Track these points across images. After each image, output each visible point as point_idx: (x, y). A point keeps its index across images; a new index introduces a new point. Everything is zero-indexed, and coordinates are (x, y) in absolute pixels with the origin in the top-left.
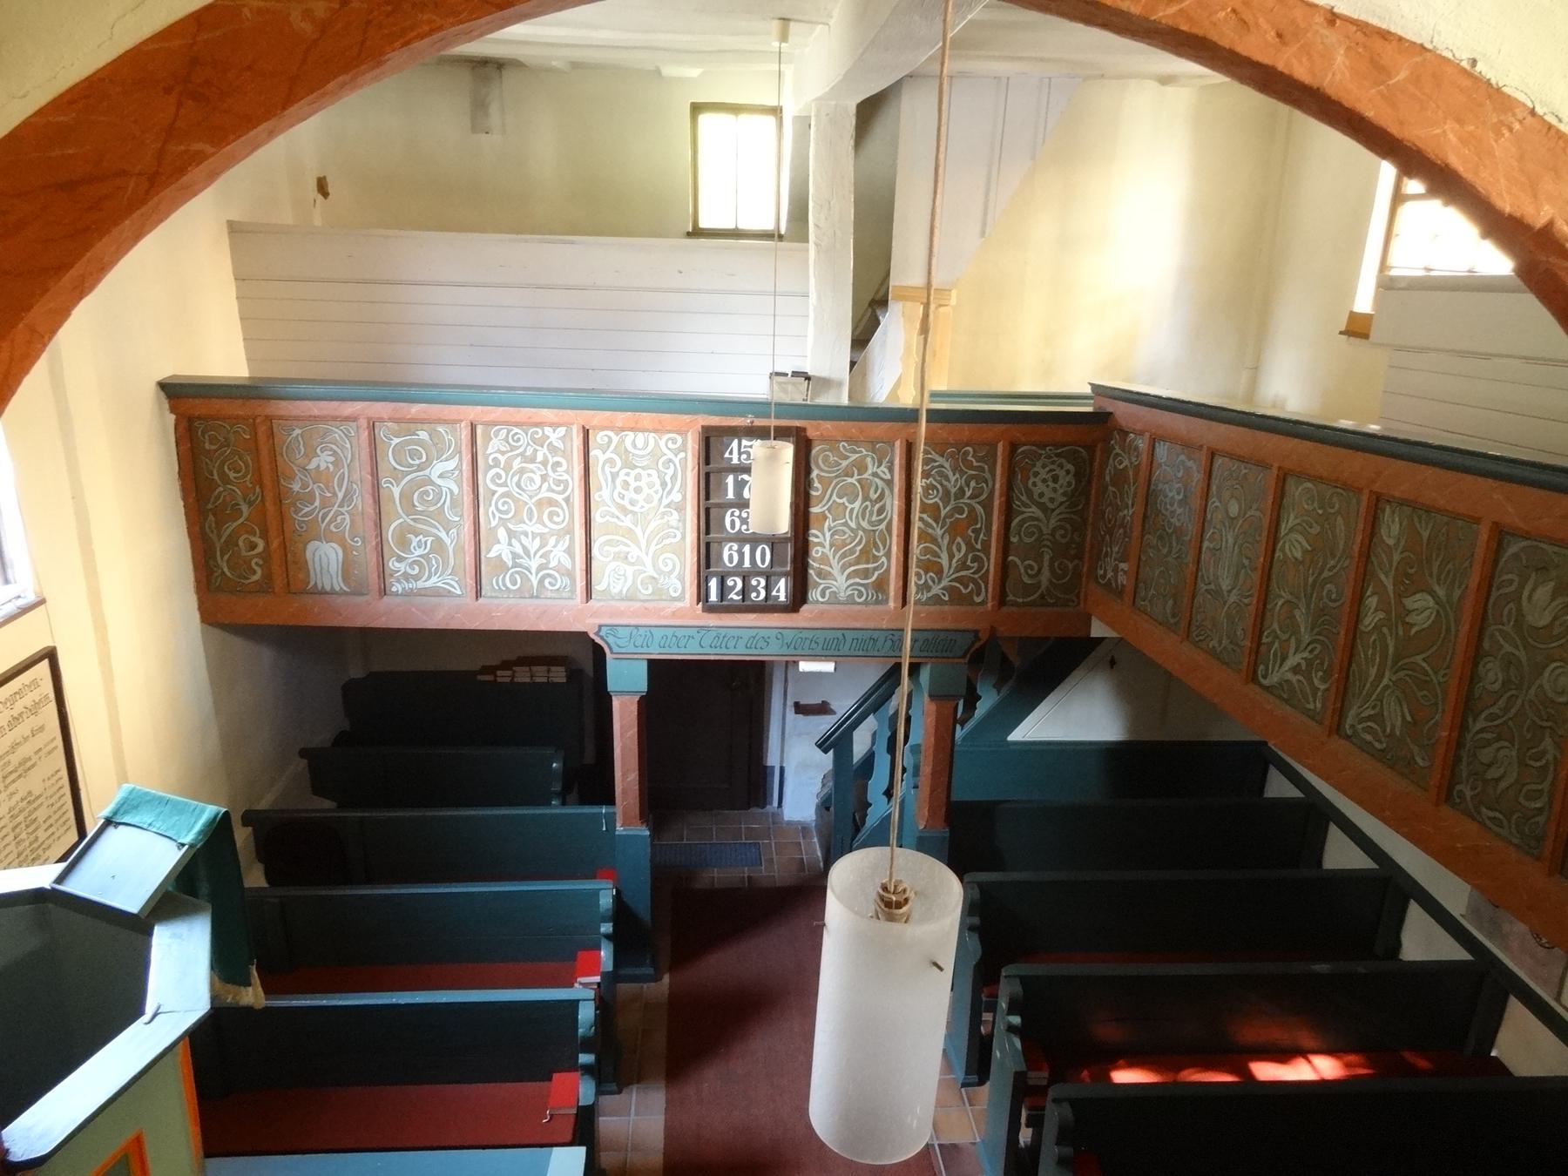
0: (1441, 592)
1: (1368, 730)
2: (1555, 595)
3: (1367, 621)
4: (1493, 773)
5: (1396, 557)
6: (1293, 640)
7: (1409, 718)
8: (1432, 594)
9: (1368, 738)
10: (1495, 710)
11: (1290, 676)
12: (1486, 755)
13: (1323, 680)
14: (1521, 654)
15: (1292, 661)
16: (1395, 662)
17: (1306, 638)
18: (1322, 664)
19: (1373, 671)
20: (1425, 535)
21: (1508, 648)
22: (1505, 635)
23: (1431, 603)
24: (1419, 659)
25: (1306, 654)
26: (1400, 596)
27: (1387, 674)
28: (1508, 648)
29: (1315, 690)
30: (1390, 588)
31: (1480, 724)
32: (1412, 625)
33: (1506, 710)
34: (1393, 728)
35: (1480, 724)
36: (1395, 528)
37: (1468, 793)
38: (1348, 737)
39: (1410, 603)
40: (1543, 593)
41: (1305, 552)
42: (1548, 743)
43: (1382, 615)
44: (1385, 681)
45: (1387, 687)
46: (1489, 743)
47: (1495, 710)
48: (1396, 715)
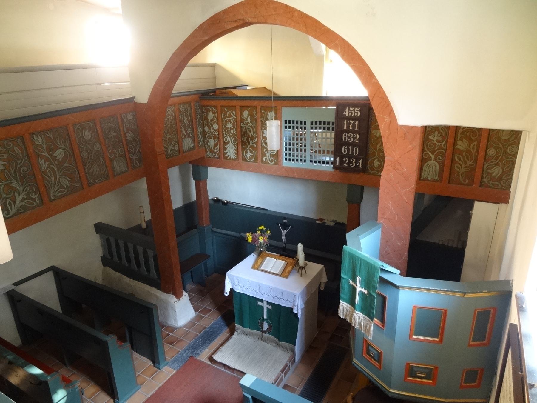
0: (63, 147)
1: (60, 192)
2: (89, 131)
3: (43, 168)
4: (94, 173)
5: (45, 146)
6: (16, 194)
7: (69, 179)
8: (60, 148)
9: (60, 194)
10: (89, 160)
11: (21, 204)
12: (91, 171)
13: (35, 194)
14: (89, 147)
15: (19, 199)
16: (58, 170)
17: (21, 189)
18: (33, 190)
19: (53, 178)
20: (51, 136)
21: (85, 147)
22: (84, 145)
23: (61, 150)
24: (65, 165)
25: (24, 193)
26: (51, 155)
27: (57, 174)
28: (85, 147)
29: (34, 200)
30: (47, 155)
31: (87, 166)
32: (59, 159)
33: (91, 159)
34: (67, 185)
35: (87, 166)
36: (40, 140)
37: (91, 181)
38: (54, 200)
39: (55, 155)
40: (87, 133)
41: (4, 165)
42: (101, 158)
43: (47, 163)
44: (58, 177)
45: (59, 179)
46: (91, 168)
47: (89, 160)
48: (65, 182)
